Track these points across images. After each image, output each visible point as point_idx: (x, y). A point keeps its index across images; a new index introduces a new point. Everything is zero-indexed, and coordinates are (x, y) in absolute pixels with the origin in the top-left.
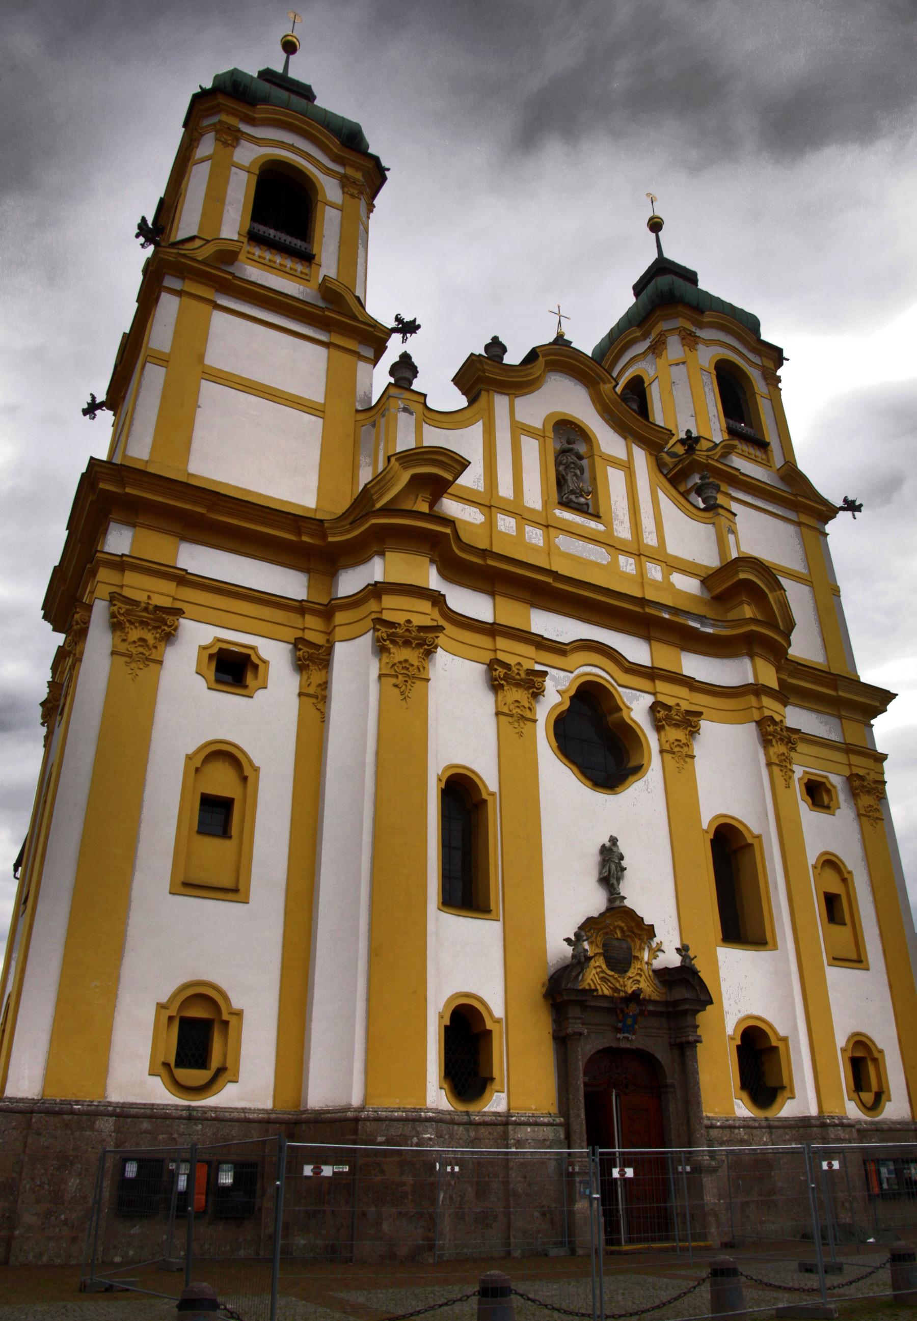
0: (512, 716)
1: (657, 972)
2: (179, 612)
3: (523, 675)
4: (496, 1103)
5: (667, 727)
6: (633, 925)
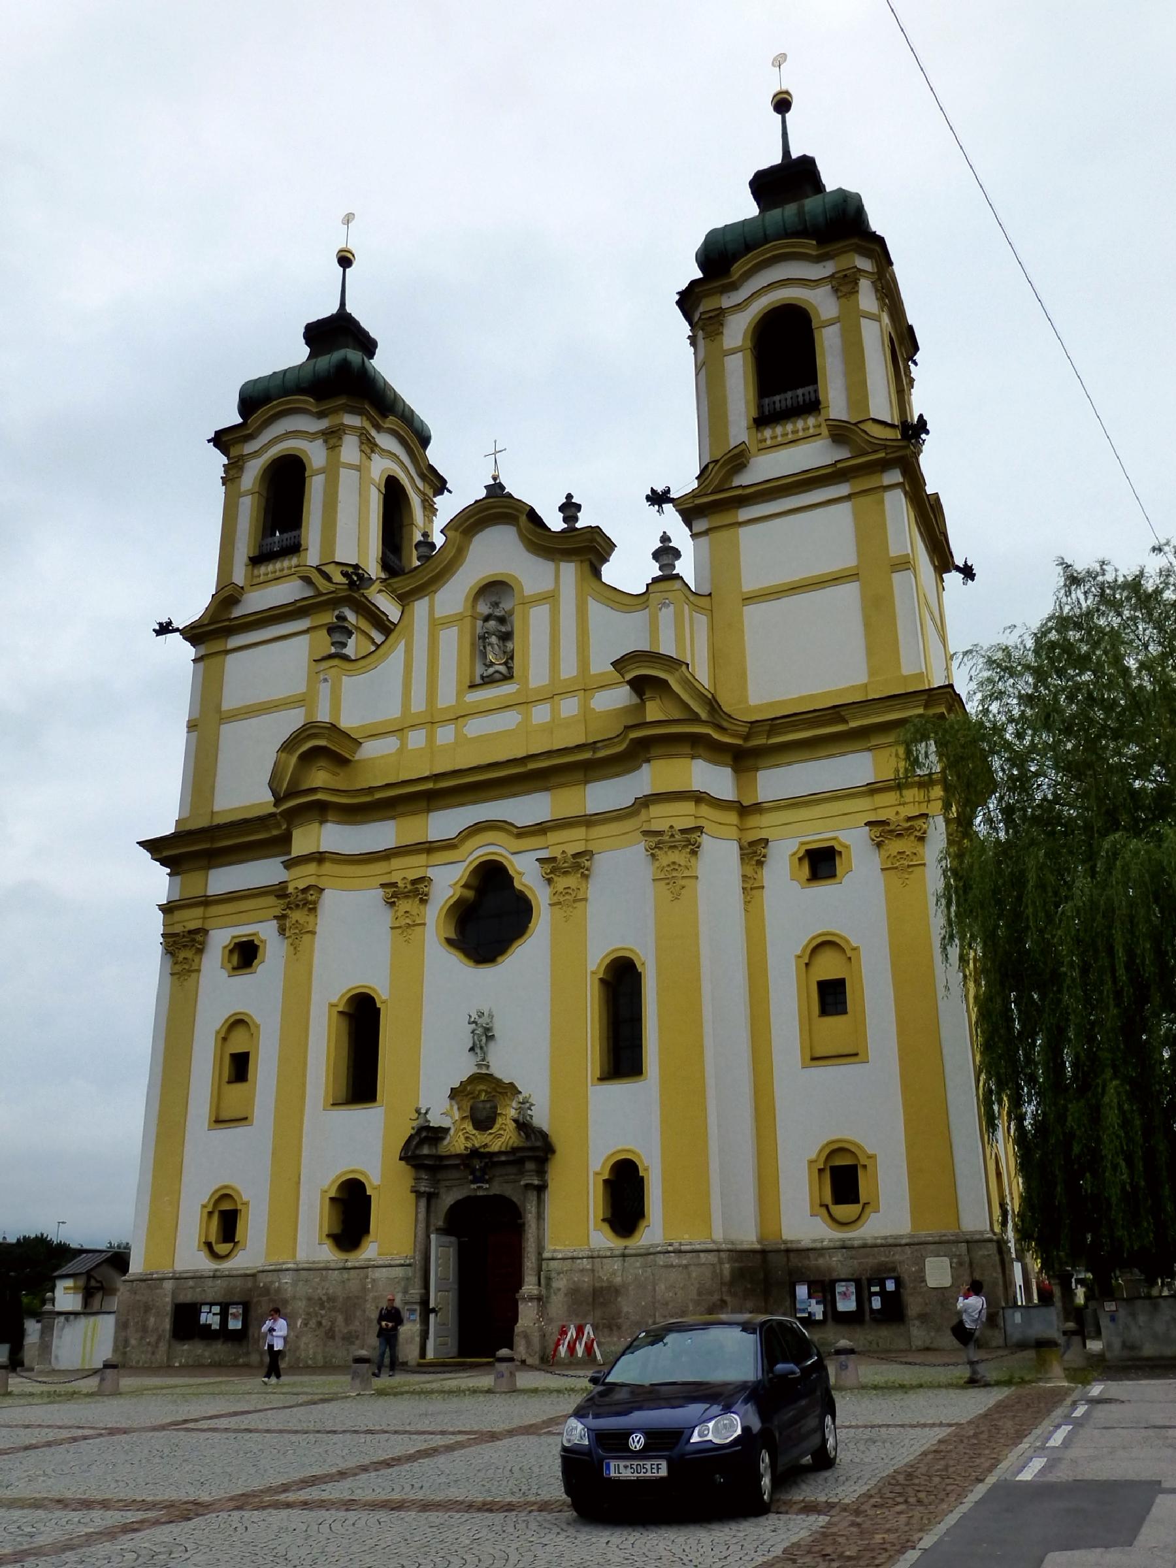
3: (409, 887)
4: (369, 1251)
5: (556, 879)
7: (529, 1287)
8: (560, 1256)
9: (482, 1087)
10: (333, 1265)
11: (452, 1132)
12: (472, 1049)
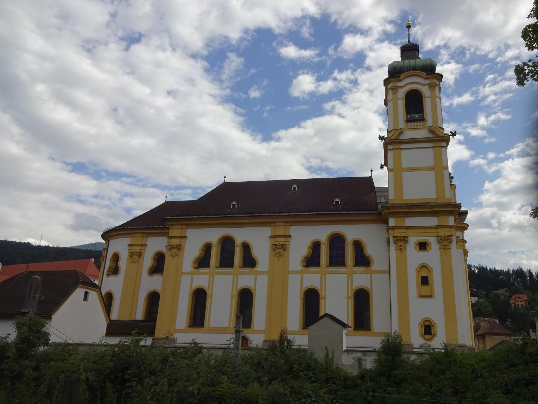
2: (407, 237)
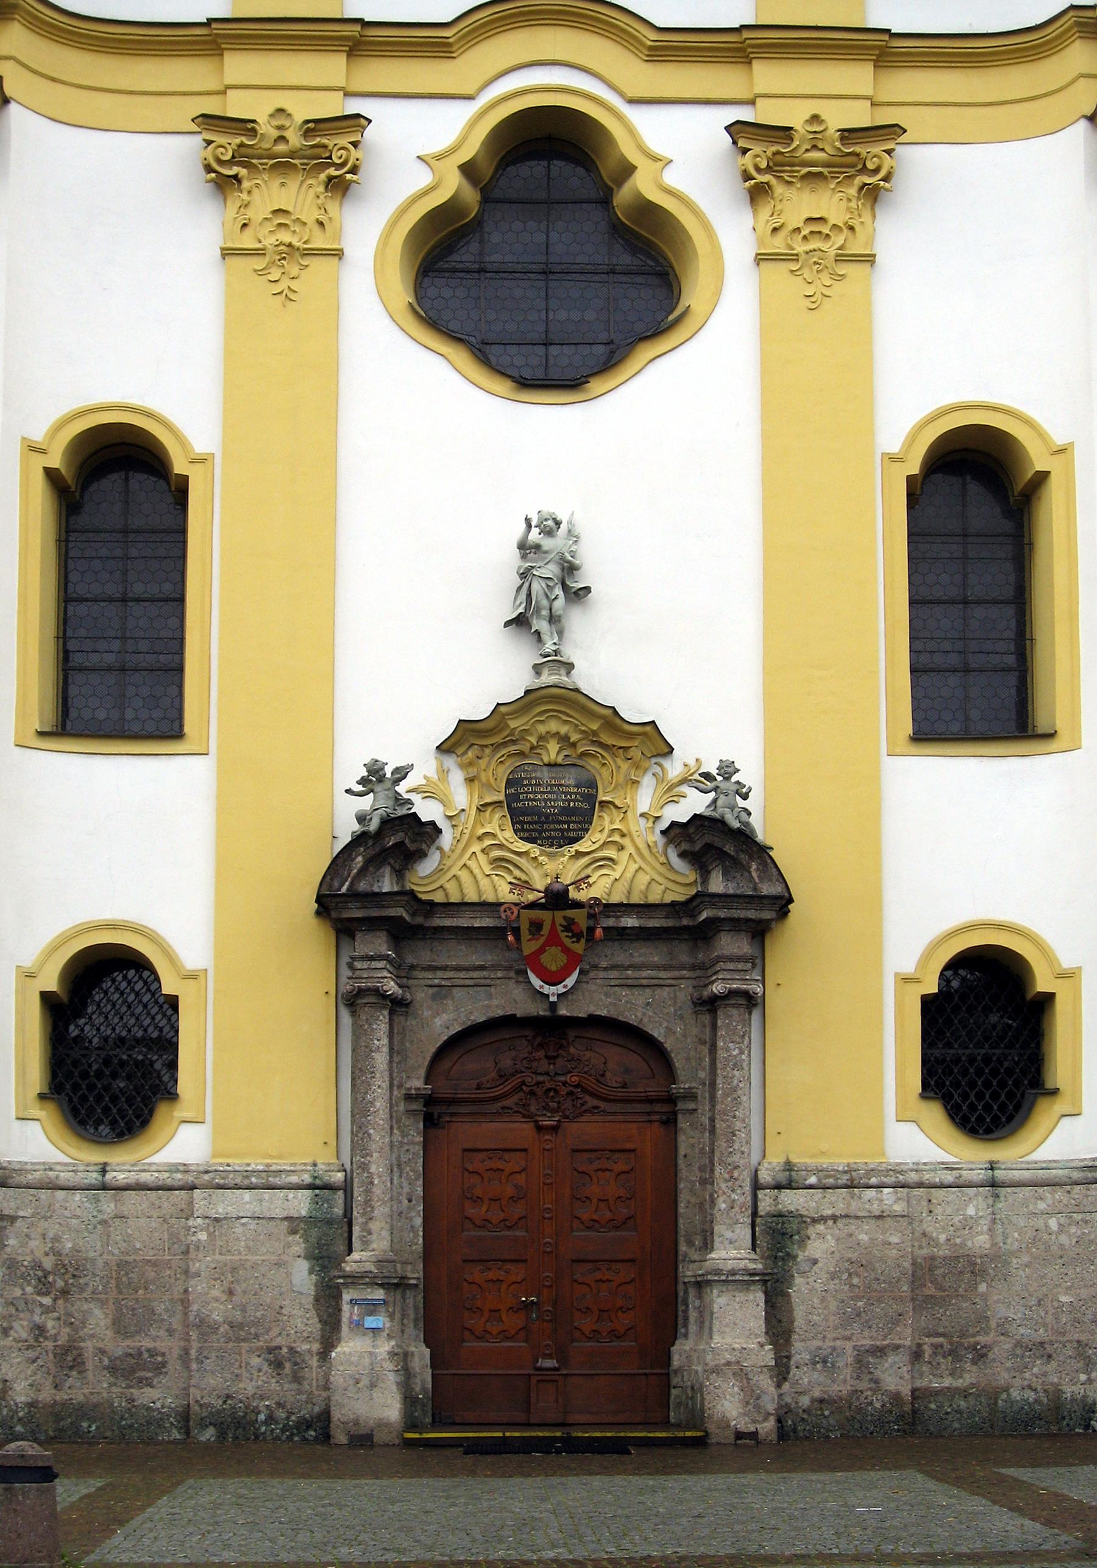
0: (259, 253)
1: (675, 832)
3: (295, 139)
4: (181, 1142)
5: (779, 189)
6: (594, 726)
7: (732, 1249)
8: (813, 1180)
9: (553, 726)
10: (65, 1177)
11: (447, 839)
12: (519, 622)
